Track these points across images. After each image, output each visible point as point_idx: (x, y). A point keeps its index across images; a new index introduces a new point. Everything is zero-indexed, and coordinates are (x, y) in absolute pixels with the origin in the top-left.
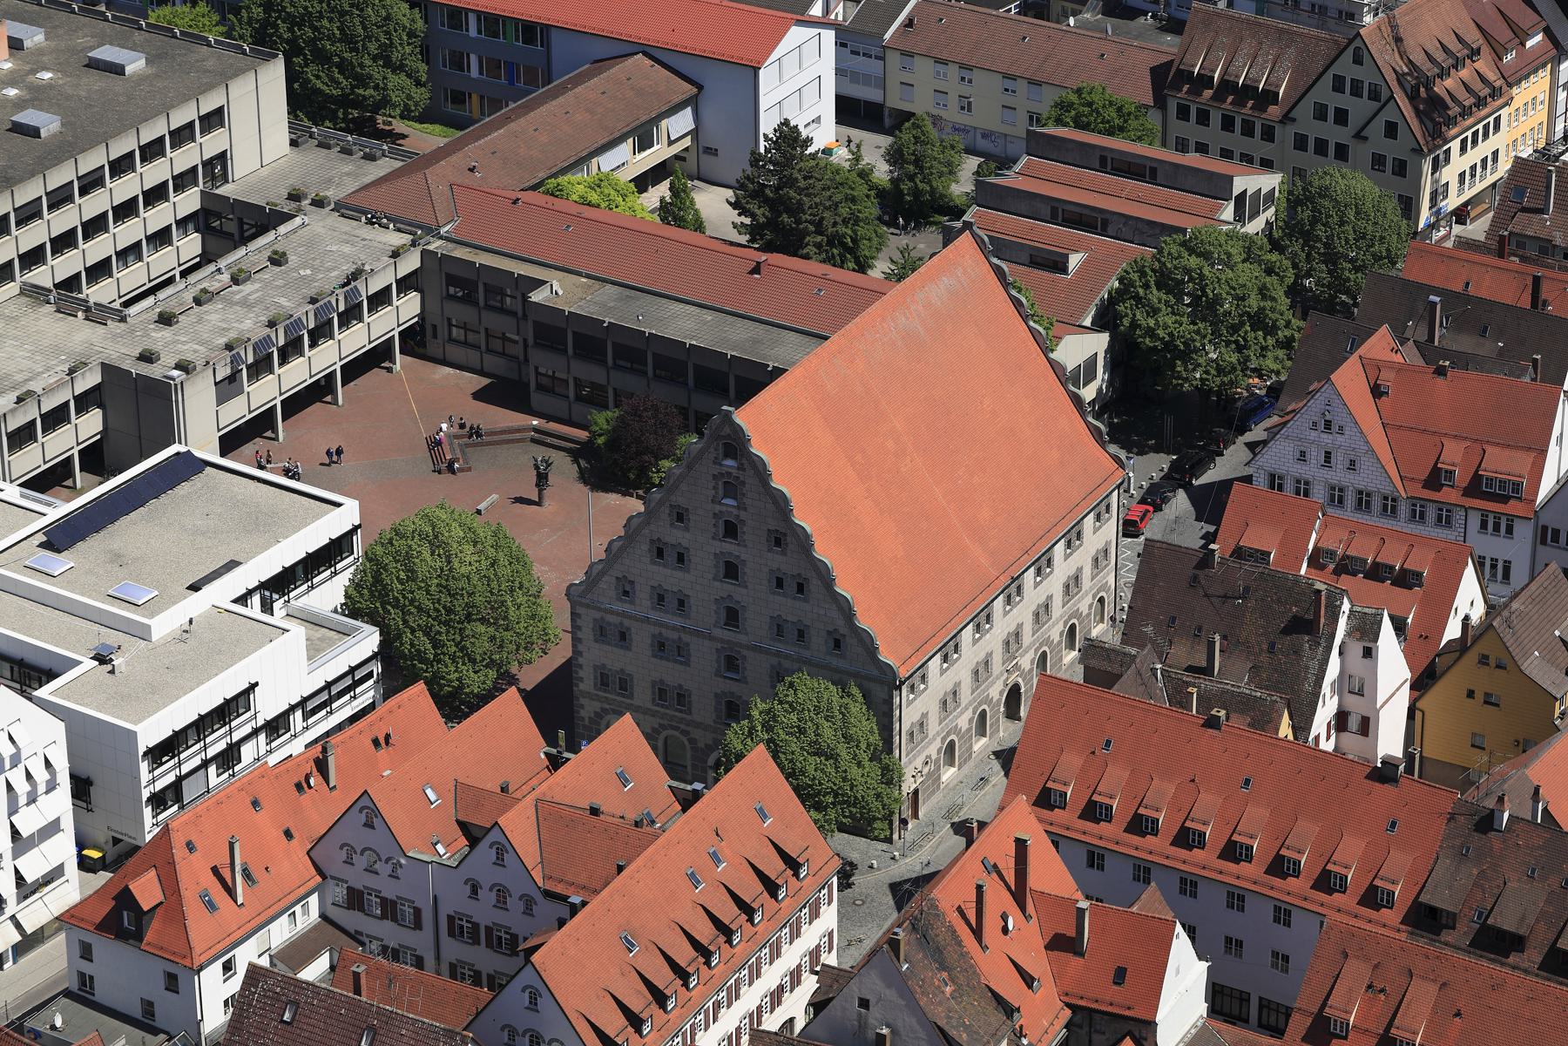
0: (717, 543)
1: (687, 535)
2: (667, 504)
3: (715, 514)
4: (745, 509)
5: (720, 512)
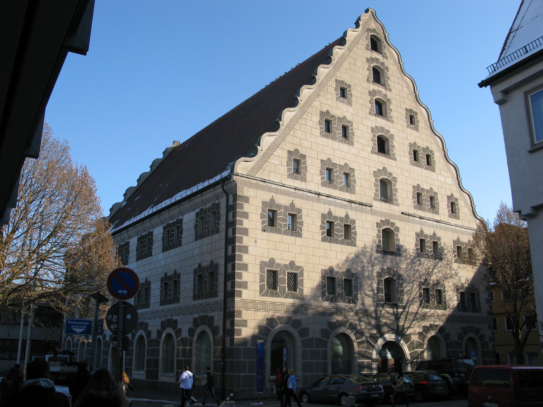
0: (373, 118)
1: (350, 109)
2: (334, 79)
3: (369, 91)
4: (390, 90)
5: (373, 90)
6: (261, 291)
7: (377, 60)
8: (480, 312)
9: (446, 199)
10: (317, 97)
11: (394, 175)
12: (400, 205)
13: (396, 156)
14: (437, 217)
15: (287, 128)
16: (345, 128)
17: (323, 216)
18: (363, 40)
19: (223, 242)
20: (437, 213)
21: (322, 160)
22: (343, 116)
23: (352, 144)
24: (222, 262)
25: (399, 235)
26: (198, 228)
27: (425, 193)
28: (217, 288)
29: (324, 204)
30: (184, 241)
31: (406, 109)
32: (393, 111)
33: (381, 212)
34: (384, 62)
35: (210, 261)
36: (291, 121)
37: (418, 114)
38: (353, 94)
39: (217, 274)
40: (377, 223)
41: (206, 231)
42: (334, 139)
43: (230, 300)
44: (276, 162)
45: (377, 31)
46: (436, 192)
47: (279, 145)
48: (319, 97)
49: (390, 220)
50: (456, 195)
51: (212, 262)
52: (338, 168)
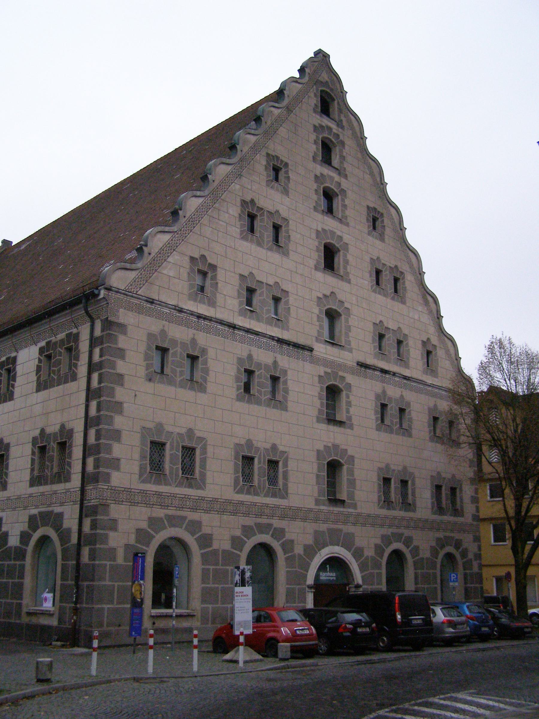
0: (319, 216)
1: (287, 200)
3: (316, 176)
4: (346, 177)
5: (322, 174)
6: (141, 475)
7: (330, 129)
8: (462, 515)
9: (419, 345)
10: (237, 177)
11: (346, 305)
12: (354, 350)
13: (351, 276)
14: (407, 373)
15: (189, 221)
16: (277, 228)
17: (240, 361)
18: (309, 97)
19: (83, 395)
20: (406, 365)
21: (241, 275)
22: (275, 210)
23: (286, 254)
24: (79, 427)
25: (351, 397)
26: (42, 372)
27: (391, 335)
28: (70, 467)
29: (242, 343)
30: (17, 391)
31: (368, 207)
32: (348, 208)
33: (325, 360)
34: (339, 133)
35: (59, 425)
36: (197, 210)
37: (385, 215)
38: (291, 177)
39: (71, 446)
40: (320, 376)
41: (56, 377)
42: (259, 244)
43: (91, 487)
44: (171, 274)
45: (331, 86)
46: (406, 333)
47: (177, 246)
48: (240, 178)
49: (337, 373)
50: (434, 340)
51: (63, 426)
52: (264, 289)
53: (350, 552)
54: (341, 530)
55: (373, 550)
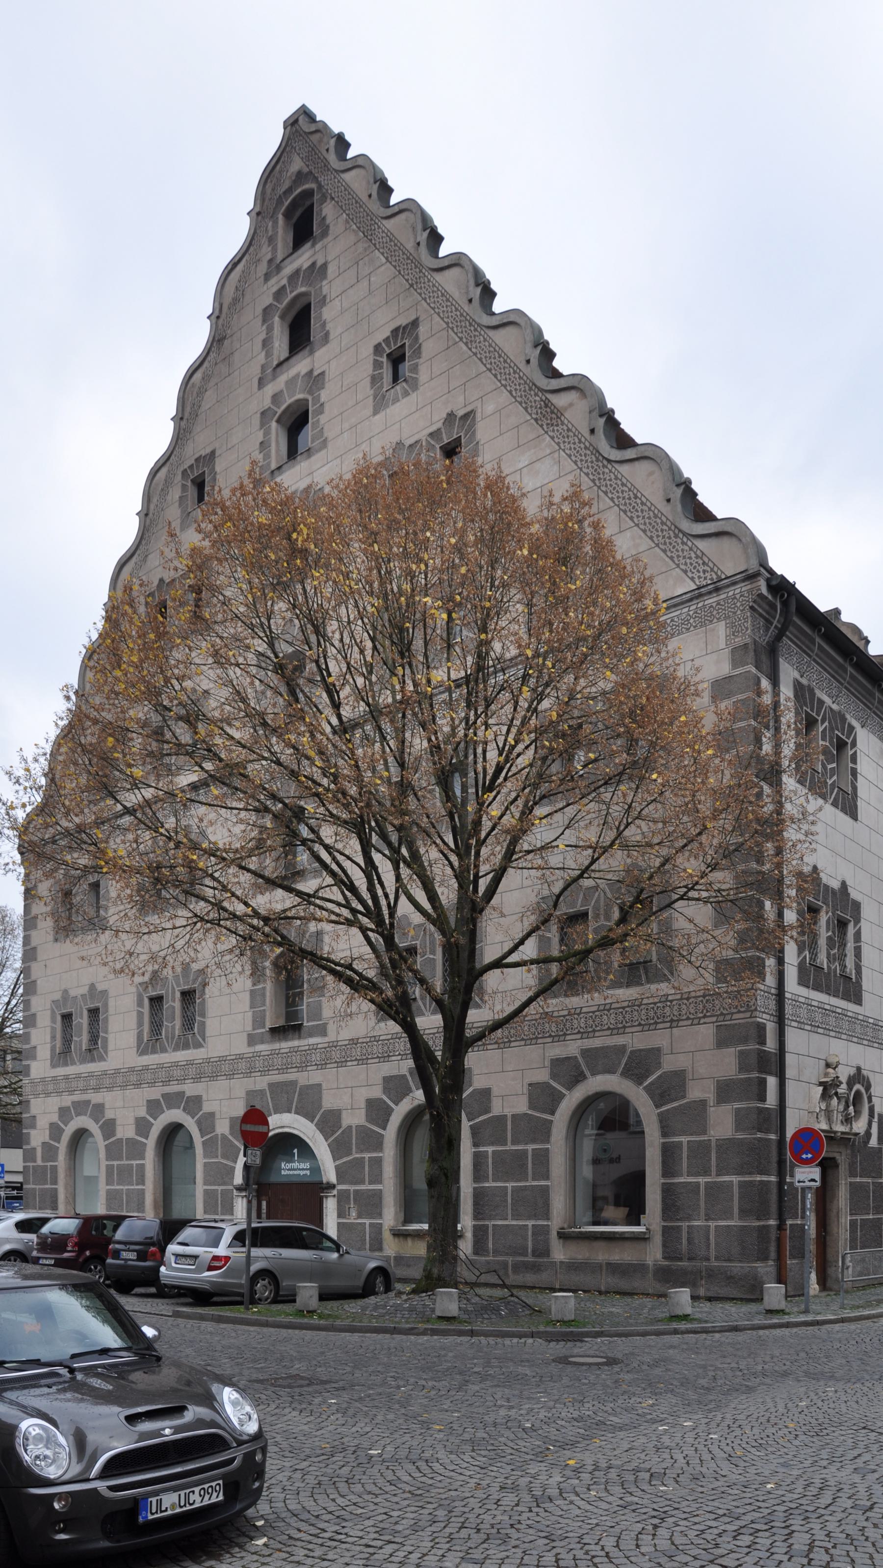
53: (312, 1121)
54: (294, 1083)
55: (363, 1111)
